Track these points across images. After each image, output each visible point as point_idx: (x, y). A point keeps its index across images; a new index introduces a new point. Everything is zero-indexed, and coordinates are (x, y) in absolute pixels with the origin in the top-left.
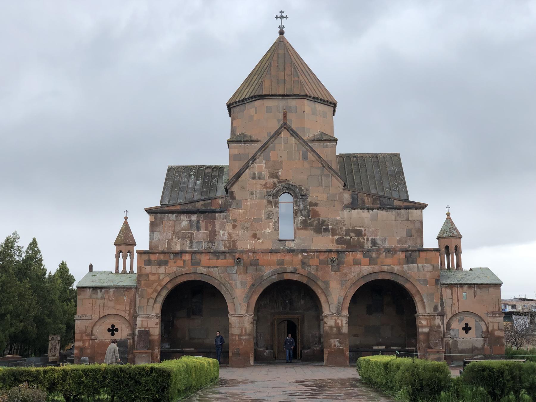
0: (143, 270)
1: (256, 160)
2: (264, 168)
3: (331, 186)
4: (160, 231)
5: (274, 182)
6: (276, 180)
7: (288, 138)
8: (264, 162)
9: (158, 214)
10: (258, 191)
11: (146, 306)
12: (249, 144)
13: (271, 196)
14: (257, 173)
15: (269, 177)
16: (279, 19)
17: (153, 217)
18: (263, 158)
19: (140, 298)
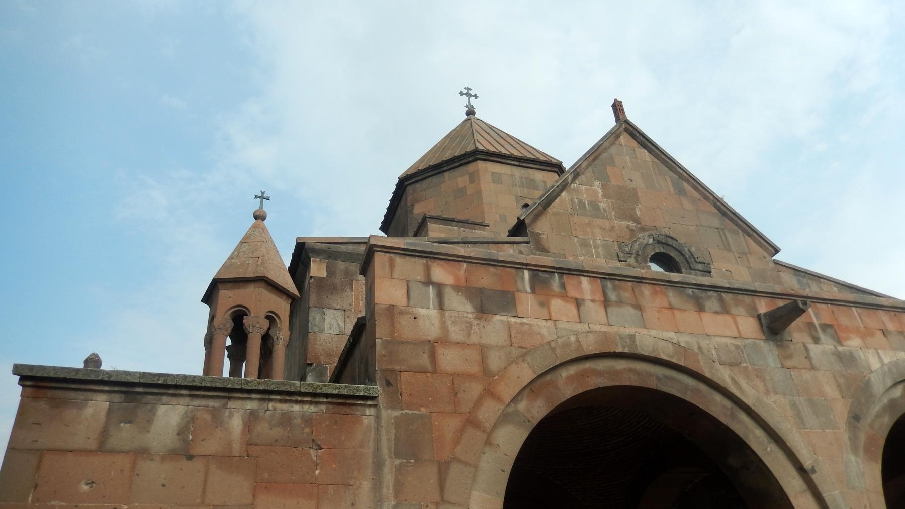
0: (404, 322)
1: (580, 178)
2: (600, 195)
3: (750, 254)
4: (346, 306)
5: (630, 227)
6: (632, 224)
7: (635, 149)
8: (596, 183)
9: (336, 259)
10: (599, 242)
11: (437, 504)
12: (468, 228)
13: (633, 256)
14: (588, 204)
15: (616, 217)
16: (464, 96)
17: (324, 266)
18: (592, 175)
19: (397, 462)
